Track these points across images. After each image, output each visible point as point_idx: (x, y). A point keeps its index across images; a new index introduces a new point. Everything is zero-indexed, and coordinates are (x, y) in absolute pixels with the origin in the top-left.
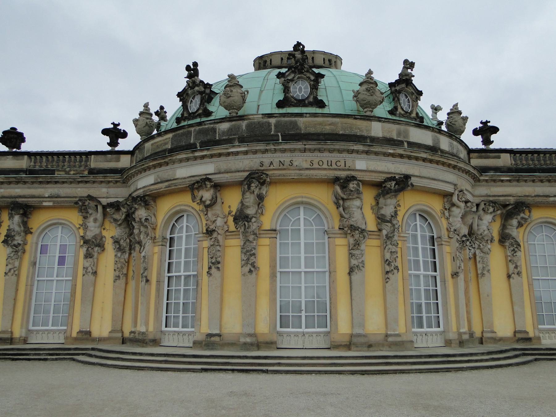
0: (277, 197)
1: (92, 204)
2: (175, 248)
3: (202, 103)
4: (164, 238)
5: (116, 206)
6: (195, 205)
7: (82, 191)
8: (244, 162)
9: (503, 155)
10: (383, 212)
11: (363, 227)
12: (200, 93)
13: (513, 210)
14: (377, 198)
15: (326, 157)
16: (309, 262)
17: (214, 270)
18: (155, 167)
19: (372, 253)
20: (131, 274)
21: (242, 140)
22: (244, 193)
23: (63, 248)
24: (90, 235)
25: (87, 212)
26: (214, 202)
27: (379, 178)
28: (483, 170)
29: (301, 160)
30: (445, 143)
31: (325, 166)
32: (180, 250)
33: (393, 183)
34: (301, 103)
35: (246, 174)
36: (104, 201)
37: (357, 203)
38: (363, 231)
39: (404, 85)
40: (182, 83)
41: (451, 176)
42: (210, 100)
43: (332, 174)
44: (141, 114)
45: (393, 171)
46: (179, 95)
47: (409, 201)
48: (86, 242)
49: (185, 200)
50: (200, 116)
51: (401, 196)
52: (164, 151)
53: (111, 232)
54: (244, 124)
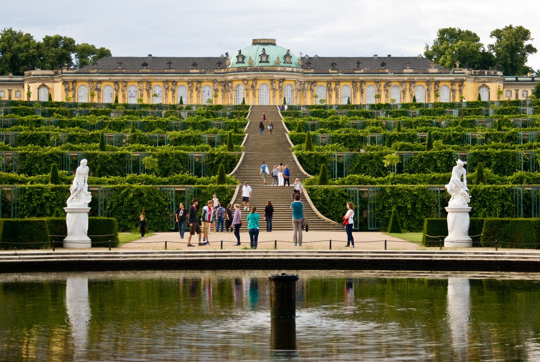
0: (259, 83)
5: (222, 82)
7: (213, 78)
8: (253, 75)
13: (313, 83)
15: (269, 75)
16: (265, 95)
19: (277, 93)
20: (226, 97)
23: (208, 91)
24: (215, 88)
26: (247, 83)
28: (307, 73)
29: (264, 76)
30: (295, 70)
34: (264, 62)
39: (288, 55)
40: (237, 53)
41: (296, 77)
47: (286, 83)
48: (215, 90)
49: (241, 82)
53: (220, 88)
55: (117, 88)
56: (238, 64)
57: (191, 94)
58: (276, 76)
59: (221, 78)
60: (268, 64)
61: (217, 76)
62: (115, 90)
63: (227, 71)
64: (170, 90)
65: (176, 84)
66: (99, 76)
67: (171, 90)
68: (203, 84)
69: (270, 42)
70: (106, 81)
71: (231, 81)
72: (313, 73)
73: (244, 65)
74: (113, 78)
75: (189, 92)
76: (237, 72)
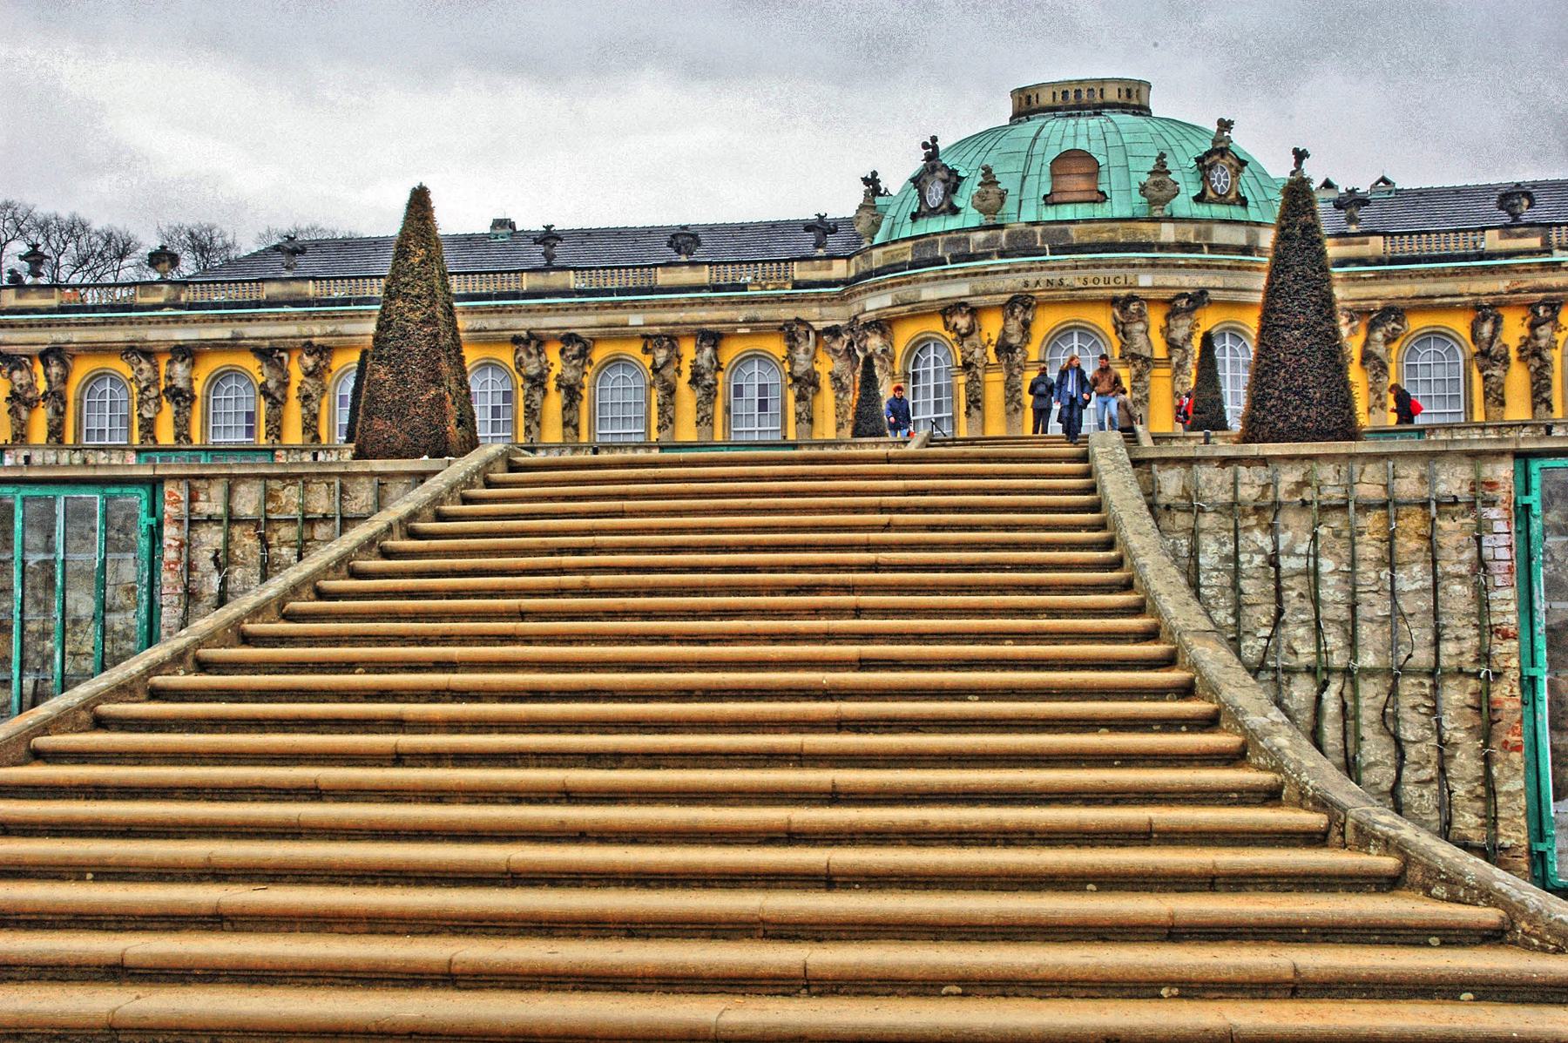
1: (802, 329)
2: (921, 385)
3: (946, 195)
4: (907, 374)
5: (834, 332)
6: (947, 334)
7: (787, 313)
9: (1372, 239)
10: (1173, 335)
11: (1148, 354)
12: (944, 181)
14: (1167, 317)
15: (1102, 273)
17: (973, 409)
18: (893, 285)
21: (1002, 255)
22: (1005, 320)
23: (763, 389)
24: (799, 370)
25: (795, 340)
26: (971, 331)
27: (1168, 295)
31: (1101, 284)
32: (926, 389)
33: (1184, 302)
35: (1008, 297)
36: (818, 326)
37: (1140, 326)
38: (1147, 360)
40: (916, 163)
42: (955, 191)
43: (1109, 293)
44: (862, 207)
45: (1186, 284)
46: (913, 180)
48: (796, 380)
49: (936, 325)
50: (943, 212)
51: (1198, 313)
52: (904, 263)
54: (1004, 233)
55: (272, 384)
56: (921, 222)
57: (662, 407)
58: (1145, 280)
59: (827, 311)
60: (1100, 211)
61: (803, 299)
62: (265, 392)
63: (863, 267)
64: (552, 385)
65: (584, 354)
66: (177, 320)
67: (559, 386)
68: (731, 352)
69: (1111, 95)
70: (219, 346)
71: (883, 325)
72: (1380, 262)
73: (953, 223)
74: (253, 331)
75: (656, 396)
76: (913, 266)
